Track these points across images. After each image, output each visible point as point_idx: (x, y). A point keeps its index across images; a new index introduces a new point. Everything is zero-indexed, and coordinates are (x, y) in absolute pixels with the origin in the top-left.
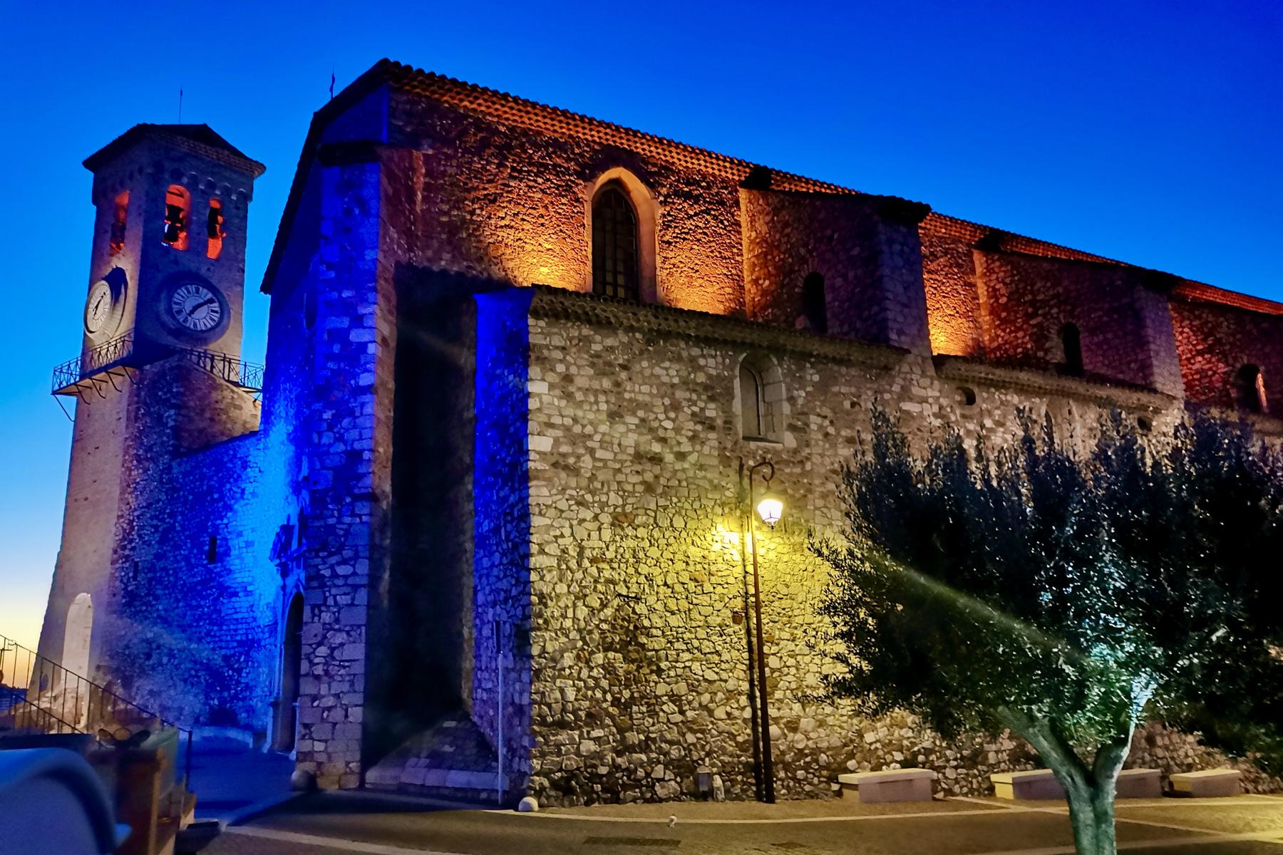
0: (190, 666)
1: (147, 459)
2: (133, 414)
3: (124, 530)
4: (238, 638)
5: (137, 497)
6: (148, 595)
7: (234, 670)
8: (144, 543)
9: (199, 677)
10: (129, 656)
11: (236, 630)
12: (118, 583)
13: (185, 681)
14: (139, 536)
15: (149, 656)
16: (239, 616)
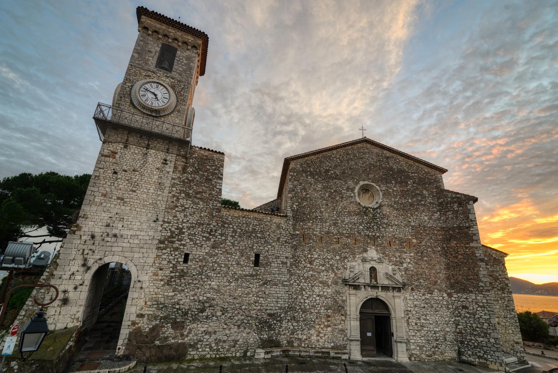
0: (242, 317)
1: (196, 197)
2: (180, 168)
3: (172, 233)
4: (279, 305)
5: (185, 216)
6: (201, 274)
7: (277, 321)
8: (195, 244)
9: (250, 324)
10: (179, 309)
11: (276, 302)
12: (165, 262)
13: (239, 327)
14: (191, 240)
15: (202, 311)
16: (279, 295)
